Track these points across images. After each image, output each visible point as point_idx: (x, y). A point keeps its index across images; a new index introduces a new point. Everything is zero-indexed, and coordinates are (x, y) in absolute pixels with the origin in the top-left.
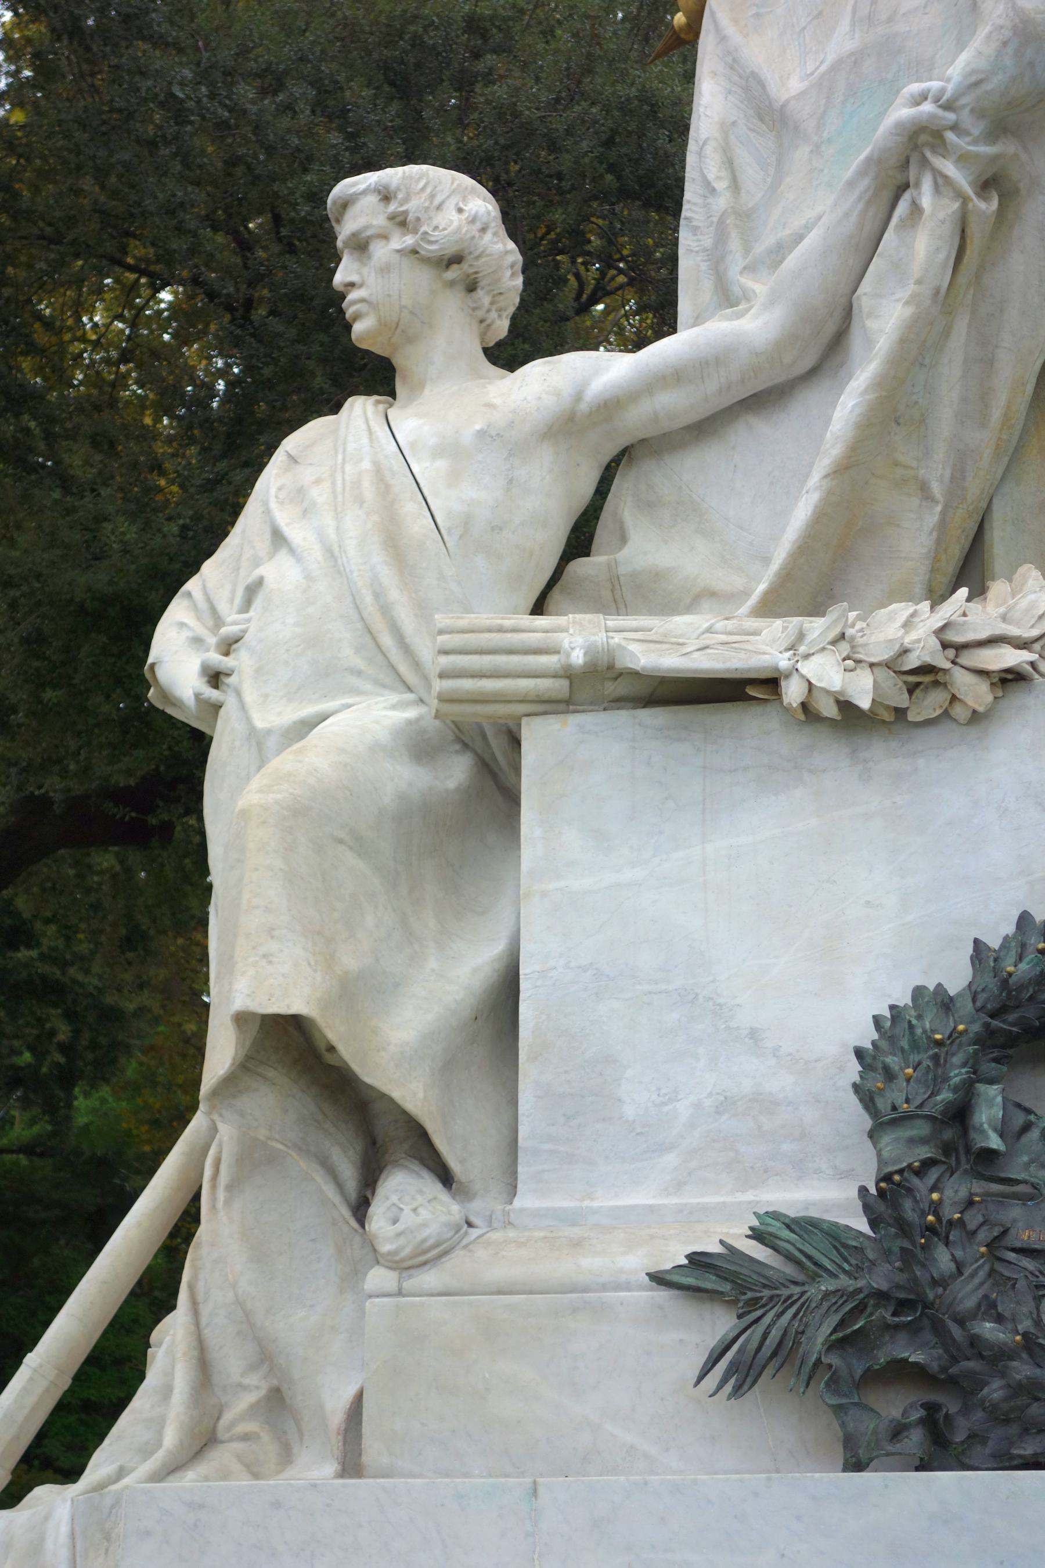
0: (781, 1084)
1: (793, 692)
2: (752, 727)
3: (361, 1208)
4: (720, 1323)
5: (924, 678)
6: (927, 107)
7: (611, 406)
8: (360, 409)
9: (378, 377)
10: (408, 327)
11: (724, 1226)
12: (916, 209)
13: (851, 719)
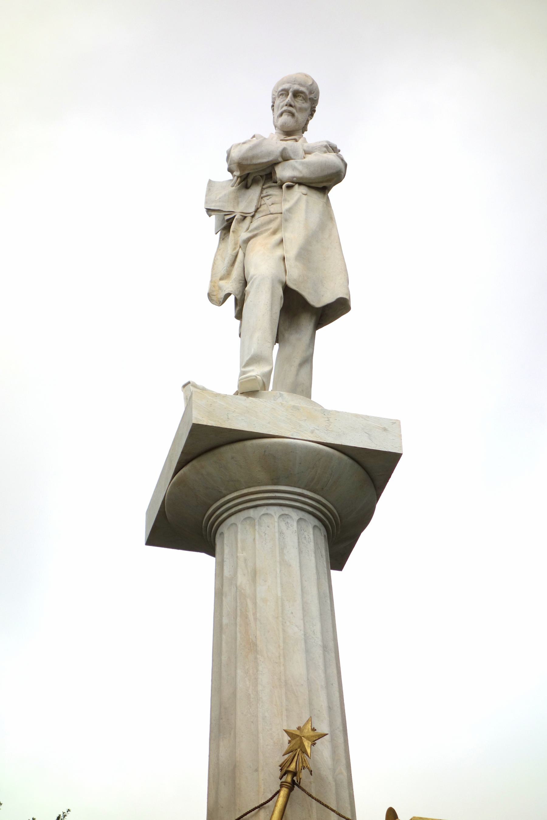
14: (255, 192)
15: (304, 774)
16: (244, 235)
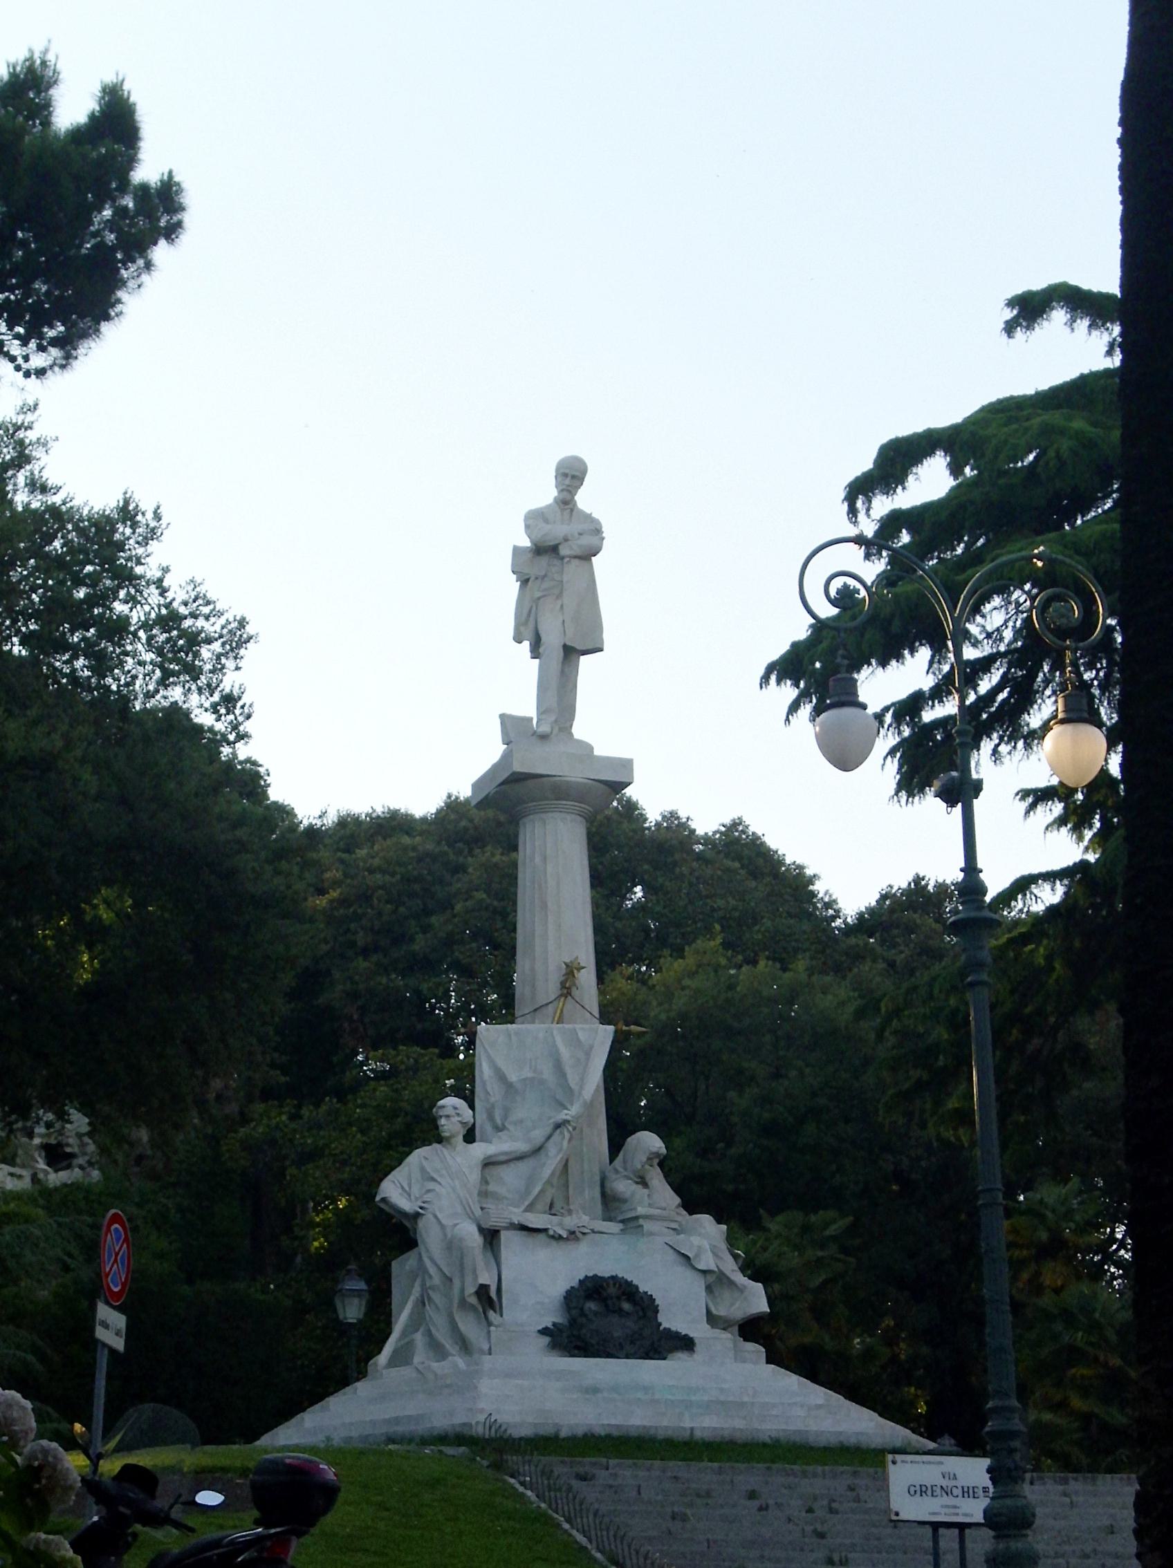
0: (547, 1300)
1: (551, 1233)
2: (542, 1236)
3: (486, 1318)
4: (547, 1340)
5: (574, 1233)
6: (568, 1118)
7: (490, 1157)
8: (436, 1145)
9: (440, 1140)
10: (452, 1136)
11: (548, 1322)
12: (562, 1133)
13: (560, 1237)
14: (544, 561)
15: (574, 989)
16: (538, 594)
